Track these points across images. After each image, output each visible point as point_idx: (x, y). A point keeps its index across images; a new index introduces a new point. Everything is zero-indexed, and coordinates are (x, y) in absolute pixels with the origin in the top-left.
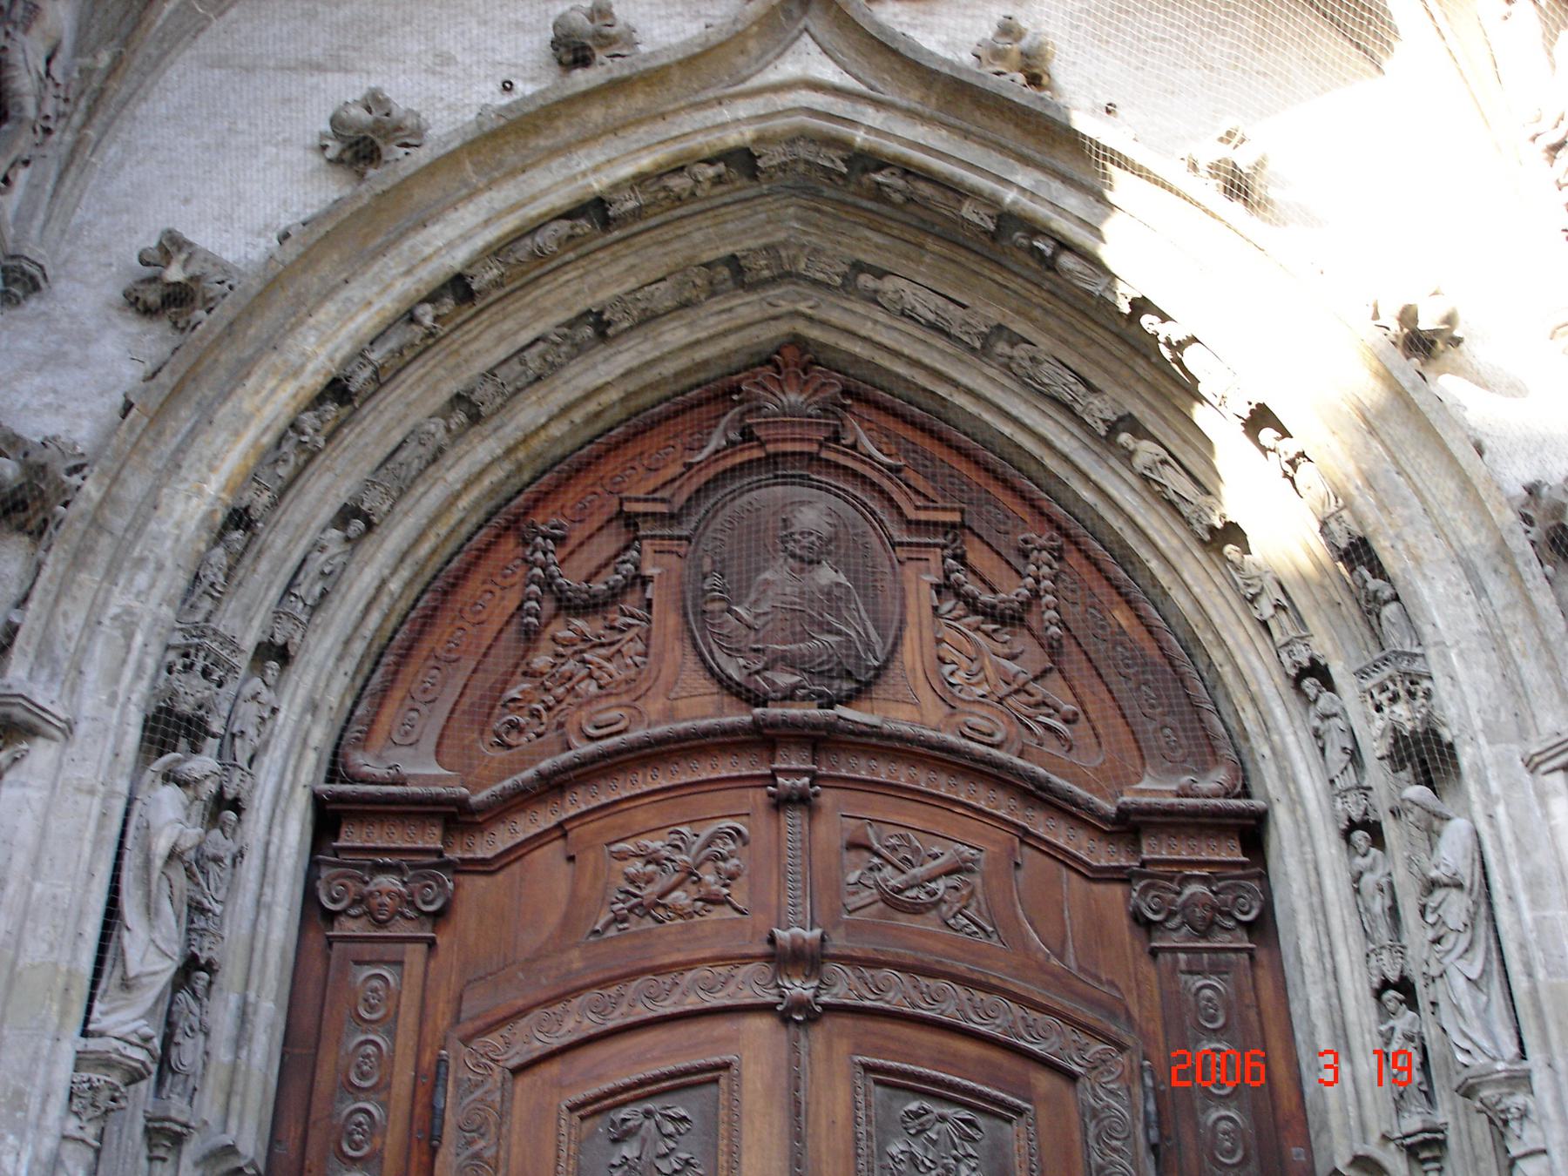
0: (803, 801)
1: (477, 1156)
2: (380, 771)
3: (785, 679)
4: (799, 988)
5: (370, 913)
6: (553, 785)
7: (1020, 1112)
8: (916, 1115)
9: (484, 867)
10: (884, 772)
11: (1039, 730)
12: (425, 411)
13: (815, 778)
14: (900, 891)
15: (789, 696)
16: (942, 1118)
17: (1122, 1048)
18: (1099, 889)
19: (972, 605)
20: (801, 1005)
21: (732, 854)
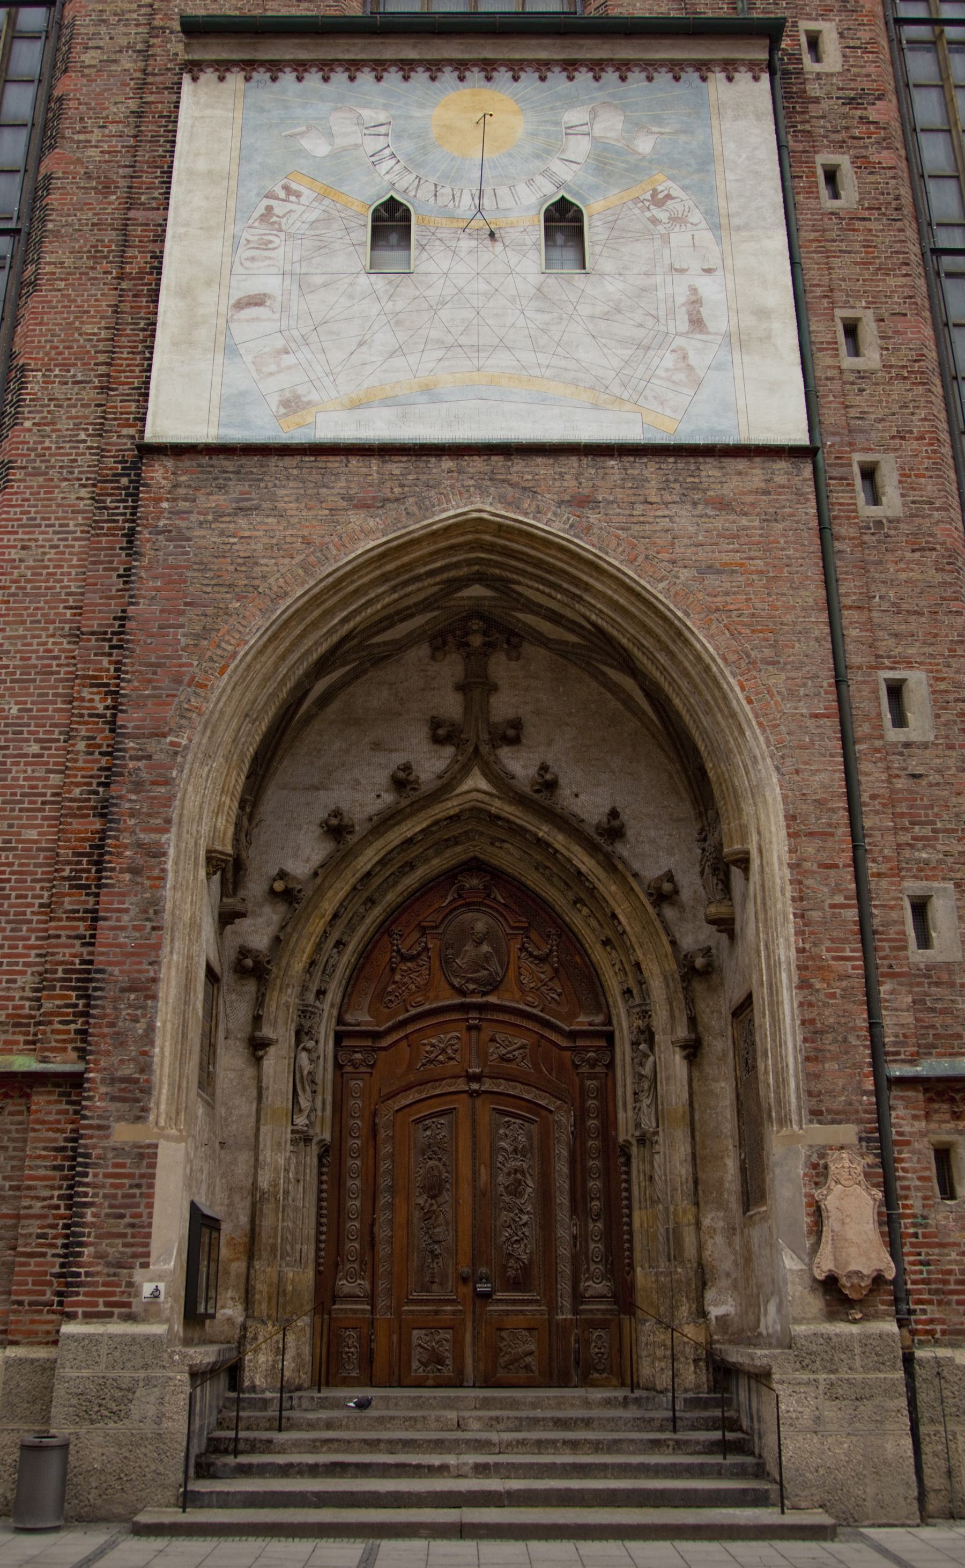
0: (477, 1028)
3: (472, 987)
4: (475, 1086)
10: (501, 1017)
13: (480, 1020)
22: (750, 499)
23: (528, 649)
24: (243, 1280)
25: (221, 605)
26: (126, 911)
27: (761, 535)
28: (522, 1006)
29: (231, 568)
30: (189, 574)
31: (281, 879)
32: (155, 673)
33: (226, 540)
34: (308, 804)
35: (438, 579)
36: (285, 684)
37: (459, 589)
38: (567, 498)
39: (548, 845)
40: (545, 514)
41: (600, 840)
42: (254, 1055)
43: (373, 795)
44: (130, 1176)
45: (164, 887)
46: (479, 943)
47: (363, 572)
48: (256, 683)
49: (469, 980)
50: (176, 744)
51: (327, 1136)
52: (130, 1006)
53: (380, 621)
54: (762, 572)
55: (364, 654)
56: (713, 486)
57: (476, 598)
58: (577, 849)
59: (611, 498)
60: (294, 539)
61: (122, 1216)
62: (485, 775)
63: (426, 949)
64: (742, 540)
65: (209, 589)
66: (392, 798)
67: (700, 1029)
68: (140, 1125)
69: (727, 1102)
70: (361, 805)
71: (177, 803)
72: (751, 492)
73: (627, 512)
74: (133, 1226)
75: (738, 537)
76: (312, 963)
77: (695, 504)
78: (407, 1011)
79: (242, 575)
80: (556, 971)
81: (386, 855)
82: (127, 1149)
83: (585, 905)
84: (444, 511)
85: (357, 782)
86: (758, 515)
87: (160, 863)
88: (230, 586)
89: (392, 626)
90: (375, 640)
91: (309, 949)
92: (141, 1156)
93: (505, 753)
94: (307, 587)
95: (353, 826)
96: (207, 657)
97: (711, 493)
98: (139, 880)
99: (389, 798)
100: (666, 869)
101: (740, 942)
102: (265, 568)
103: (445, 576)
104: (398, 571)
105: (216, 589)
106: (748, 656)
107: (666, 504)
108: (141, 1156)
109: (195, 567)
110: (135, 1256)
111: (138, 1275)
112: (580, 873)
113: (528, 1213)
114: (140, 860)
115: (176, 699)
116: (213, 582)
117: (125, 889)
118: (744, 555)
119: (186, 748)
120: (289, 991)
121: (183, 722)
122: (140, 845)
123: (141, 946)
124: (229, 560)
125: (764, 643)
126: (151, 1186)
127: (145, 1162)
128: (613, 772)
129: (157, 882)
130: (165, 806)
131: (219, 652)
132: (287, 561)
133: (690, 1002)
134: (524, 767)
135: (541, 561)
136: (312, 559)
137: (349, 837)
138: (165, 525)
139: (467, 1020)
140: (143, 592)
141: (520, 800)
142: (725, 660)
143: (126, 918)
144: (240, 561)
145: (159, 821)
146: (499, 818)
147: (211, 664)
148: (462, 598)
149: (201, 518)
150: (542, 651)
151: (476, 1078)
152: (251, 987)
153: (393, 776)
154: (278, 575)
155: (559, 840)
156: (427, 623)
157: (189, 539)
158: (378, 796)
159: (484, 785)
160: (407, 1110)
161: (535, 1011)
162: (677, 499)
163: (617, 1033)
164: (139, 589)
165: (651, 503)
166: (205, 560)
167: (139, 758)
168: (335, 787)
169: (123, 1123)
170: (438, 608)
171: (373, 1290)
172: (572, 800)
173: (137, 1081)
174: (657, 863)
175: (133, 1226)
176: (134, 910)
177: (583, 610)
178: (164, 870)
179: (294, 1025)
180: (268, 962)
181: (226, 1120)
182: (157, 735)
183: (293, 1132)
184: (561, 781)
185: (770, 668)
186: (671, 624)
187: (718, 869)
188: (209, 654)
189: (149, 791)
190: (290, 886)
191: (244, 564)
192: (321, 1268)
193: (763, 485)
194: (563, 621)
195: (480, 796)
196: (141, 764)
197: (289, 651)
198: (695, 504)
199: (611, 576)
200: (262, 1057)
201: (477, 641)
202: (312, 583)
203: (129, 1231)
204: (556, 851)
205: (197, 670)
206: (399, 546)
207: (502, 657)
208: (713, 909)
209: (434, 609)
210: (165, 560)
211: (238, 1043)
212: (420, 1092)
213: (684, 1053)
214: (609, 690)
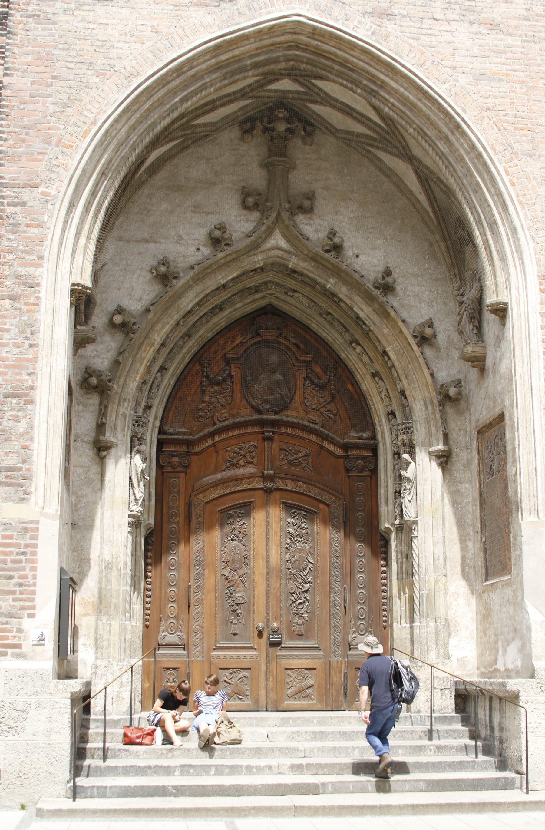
0: (270, 439)
1: (199, 521)
2: (171, 431)
3: (267, 406)
4: (269, 485)
5: (172, 466)
6: (212, 435)
7: (316, 513)
8: (293, 513)
9: (196, 454)
10: (289, 431)
11: (327, 417)
12: (178, 338)
13: (273, 433)
14: (292, 461)
15: (268, 411)
16: (299, 514)
17: (339, 499)
18: (338, 460)
19: (313, 383)
20: (268, 488)
21: (254, 451)
22: (514, 22)
23: (319, 136)
24: (93, 631)
25: (83, 80)
26: (8, 331)
27: (522, 53)
28: (307, 423)
29: (92, 49)
30: (56, 52)
31: (119, 313)
32: (27, 134)
33: (87, 26)
34: (140, 254)
35: (260, 70)
36: (134, 150)
37: (271, 82)
38: (369, 10)
39: (334, 295)
40: (352, 22)
41: (375, 292)
42: (98, 455)
43: (194, 248)
44: (18, 546)
45: (39, 312)
46: (273, 372)
47: (202, 60)
48: (112, 147)
49: (265, 401)
50: (48, 195)
51: (152, 521)
52: (12, 409)
53: (206, 104)
54: (523, 82)
55: (189, 132)
56: (485, 10)
57: (282, 91)
58: (357, 299)
59: (405, 13)
60: (144, 28)
61: (11, 577)
62: (284, 236)
63: (230, 376)
64: (509, 55)
65: (72, 66)
66: (209, 251)
67: (451, 442)
68: (23, 505)
69: (470, 499)
70: (183, 256)
71: (48, 242)
72: (515, 18)
73: (418, 25)
74: (21, 585)
75: (504, 52)
76: (144, 383)
77: (471, 23)
78: (215, 424)
79: (101, 55)
80: (333, 397)
81: (203, 298)
82: (13, 524)
83: (359, 344)
84: (269, 13)
85: (181, 238)
86: (520, 36)
87: (35, 292)
88: (90, 64)
89: (216, 108)
90: (197, 122)
91: (142, 370)
92: (26, 530)
93: (300, 219)
94: (156, 69)
95: (178, 273)
96: (71, 122)
97: (483, 15)
98: (17, 305)
99: (206, 251)
100: (426, 318)
101: (491, 375)
102: (120, 51)
103: (266, 69)
104: (227, 64)
105: (79, 65)
106: (512, 148)
107: (449, 21)
108: (26, 530)
109: (61, 46)
110: (23, 608)
111: (26, 623)
112: (358, 317)
113: (309, 582)
114: (18, 289)
115: (46, 156)
116: (76, 60)
117: (6, 313)
118: (509, 67)
119: (55, 197)
120: (126, 404)
121: (52, 175)
122: (18, 277)
123: (20, 360)
124: (89, 42)
125: (524, 139)
126: (34, 554)
127: (28, 534)
128: (386, 239)
129: (33, 308)
130: (38, 245)
131: (82, 118)
132: (138, 46)
133: (445, 421)
134: (316, 231)
135: (346, 61)
136: (159, 45)
137: (175, 281)
138: (34, 10)
139: (263, 433)
140: (16, 65)
141: (314, 258)
142: (494, 150)
143: (6, 336)
144: (100, 44)
145: (33, 257)
146: (294, 271)
147: (76, 129)
148: (271, 91)
149: (65, 6)
150: (332, 139)
151: (271, 478)
152: (95, 400)
153: (210, 234)
154: (131, 57)
155: (343, 292)
156: (239, 110)
157: (54, 23)
158: (198, 249)
159: (283, 244)
160: (215, 502)
161: (317, 427)
162: (457, 17)
163: (381, 446)
164: (13, 63)
165: (437, 20)
166: (69, 41)
167: (15, 205)
168: (162, 240)
169: (10, 503)
170: (252, 97)
171: (188, 640)
172: (354, 260)
173: (20, 470)
174: (420, 312)
175: (21, 585)
176: (14, 331)
177: (377, 103)
178: (38, 298)
179: (130, 431)
180: (110, 381)
181: (76, 506)
182: (30, 186)
183: (130, 516)
184: (345, 244)
185: (528, 158)
186: (451, 118)
187: (474, 317)
188: (73, 120)
189: (24, 232)
190: (127, 319)
191: (102, 46)
192: (147, 623)
193: (524, 12)
194: (354, 114)
195: (280, 253)
196: (18, 209)
197: (139, 122)
198: (471, 23)
199: (404, 76)
200: (105, 457)
201: (281, 127)
202: (160, 65)
203: (18, 589)
204: (340, 300)
205: (63, 133)
206: (232, 40)
207: (299, 142)
208: (469, 349)
209: (249, 98)
210: (34, 40)
211: (85, 445)
212: (225, 489)
213: (439, 462)
214: (384, 173)
